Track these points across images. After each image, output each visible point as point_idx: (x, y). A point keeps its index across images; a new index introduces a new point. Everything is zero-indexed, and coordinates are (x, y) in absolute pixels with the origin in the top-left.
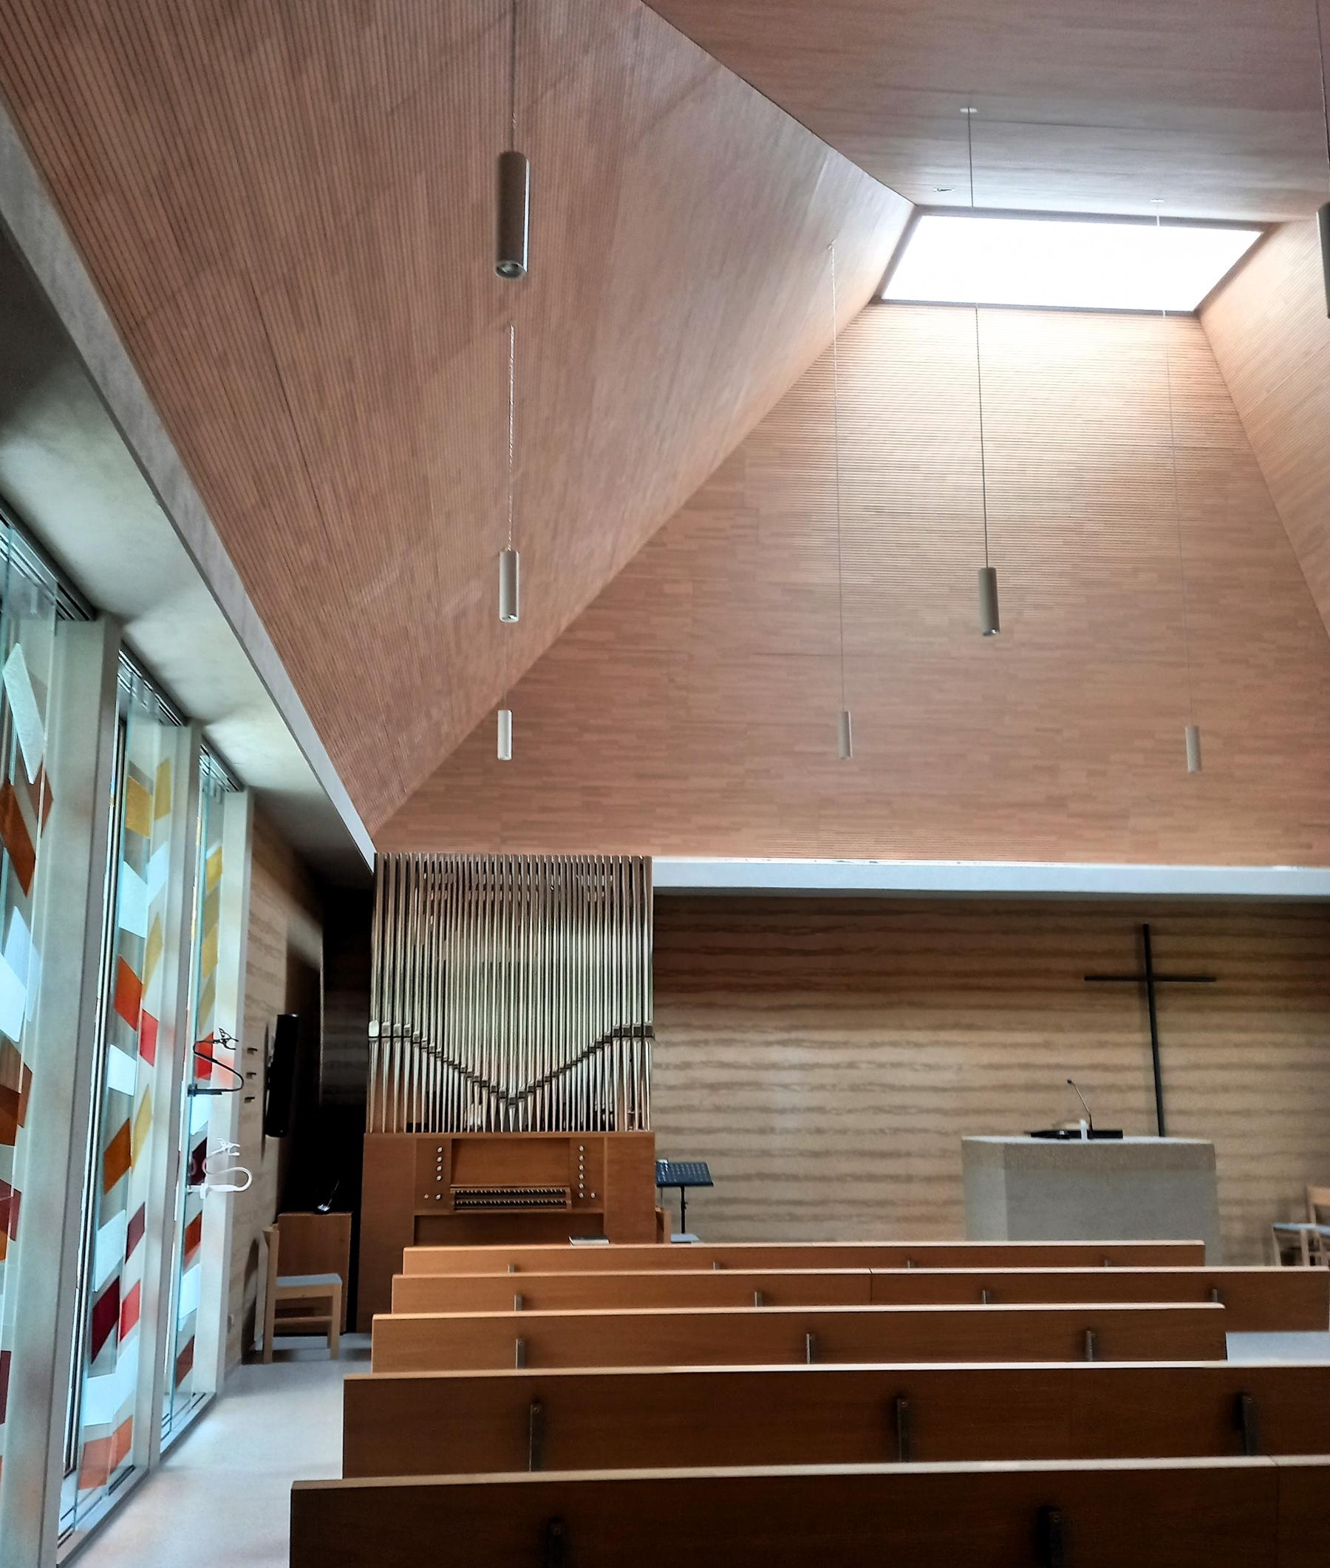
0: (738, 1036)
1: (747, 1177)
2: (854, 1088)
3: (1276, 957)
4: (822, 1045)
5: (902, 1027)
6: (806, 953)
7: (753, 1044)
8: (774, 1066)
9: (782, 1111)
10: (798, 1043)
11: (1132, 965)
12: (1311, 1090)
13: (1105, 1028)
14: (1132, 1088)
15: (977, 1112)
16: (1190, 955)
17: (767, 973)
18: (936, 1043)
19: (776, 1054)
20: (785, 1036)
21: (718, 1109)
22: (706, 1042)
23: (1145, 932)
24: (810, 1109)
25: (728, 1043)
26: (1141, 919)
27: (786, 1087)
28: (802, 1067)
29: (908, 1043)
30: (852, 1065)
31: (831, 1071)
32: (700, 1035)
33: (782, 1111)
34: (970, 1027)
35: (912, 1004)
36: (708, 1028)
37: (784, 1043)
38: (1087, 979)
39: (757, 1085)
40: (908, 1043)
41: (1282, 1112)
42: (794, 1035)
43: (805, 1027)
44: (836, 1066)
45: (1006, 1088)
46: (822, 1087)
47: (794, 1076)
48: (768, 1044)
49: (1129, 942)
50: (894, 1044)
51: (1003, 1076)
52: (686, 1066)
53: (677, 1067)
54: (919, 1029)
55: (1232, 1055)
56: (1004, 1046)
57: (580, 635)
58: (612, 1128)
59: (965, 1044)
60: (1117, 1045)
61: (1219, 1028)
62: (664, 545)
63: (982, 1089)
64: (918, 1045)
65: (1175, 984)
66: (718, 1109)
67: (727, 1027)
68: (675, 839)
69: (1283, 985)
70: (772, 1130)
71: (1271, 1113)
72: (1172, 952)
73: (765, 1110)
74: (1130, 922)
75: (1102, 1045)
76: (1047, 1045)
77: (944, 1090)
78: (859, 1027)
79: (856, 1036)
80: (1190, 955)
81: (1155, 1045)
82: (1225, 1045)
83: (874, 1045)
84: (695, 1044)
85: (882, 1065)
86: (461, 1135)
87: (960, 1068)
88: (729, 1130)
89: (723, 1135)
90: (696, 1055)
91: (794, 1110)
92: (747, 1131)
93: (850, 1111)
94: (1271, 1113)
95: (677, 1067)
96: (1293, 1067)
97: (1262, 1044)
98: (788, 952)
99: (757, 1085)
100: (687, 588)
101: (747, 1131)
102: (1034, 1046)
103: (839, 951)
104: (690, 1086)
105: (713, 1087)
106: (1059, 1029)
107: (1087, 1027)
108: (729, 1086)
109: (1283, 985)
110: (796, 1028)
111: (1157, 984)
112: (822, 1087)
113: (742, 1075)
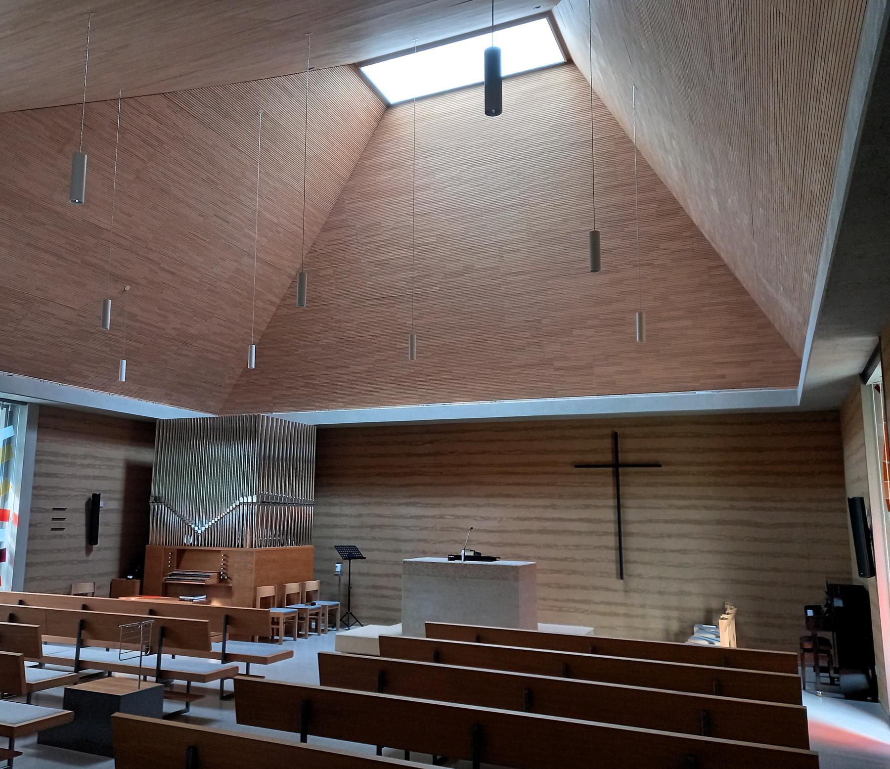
0: (385, 501)
1: (387, 575)
2: (443, 529)
3: (712, 450)
4: (426, 505)
5: (470, 496)
6: (420, 455)
7: (392, 504)
8: (402, 517)
9: (406, 541)
10: (414, 504)
11: (608, 457)
12: (733, 538)
13: (589, 496)
14: (606, 534)
15: (511, 545)
16: (649, 450)
17: (400, 467)
18: (488, 505)
19: (403, 510)
20: (408, 500)
21: (374, 539)
22: (370, 504)
23: (615, 436)
24: (419, 540)
25: (380, 504)
26: (614, 429)
27: (407, 528)
28: (417, 517)
29: (473, 504)
30: (442, 517)
31: (431, 520)
32: (367, 500)
33: (406, 541)
34: (508, 496)
35: (477, 483)
36: (370, 496)
37: (407, 504)
38: (576, 466)
39: (394, 527)
40: (473, 504)
41: (709, 552)
42: (413, 500)
43: (419, 496)
44: (433, 517)
45: (528, 531)
46: (426, 528)
47: (412, 522)
48: (400, 505)
49: (608, 443)
50: (465, 505)
51: (527, 525)
52: (361, 515)
53: (356, 516)
54: (478, 496)
55: (673, 514)
56: (528, 507)
57: (288, 301)
58: (242, 546)
59: (505, 506)
60: (596, 507)
61: (668, 497)
62: (316, 251)
63: (513, 531)
64: (478, 506)
65: (636, 469)
66: (374, 539)
67: (379, 496)
68: (350, 399)
69: (714, 468)
70: (400, 551)
71: (702, 552)
72: (630, 451)
73: (397, 540)
74: (608, 431)
75: (587, 507)
76: (553, 507)
77: (492, 532)
78: (448, 495)
79: (445, 501)
80: (649, 450)
81: (619, 507)
82: (670, 507)
83: (454, 506)
84: (364, 504)
85: (458, 517)
86: (183, 547)
87: (501, 519)
88: (379, 550)
89: (377, 553)
90: (364, 510)
91: (411, 540)
92: (388, 551)
93: (441, 542)
94: (702, 552)
95: (356, 516)
96: (719, 522)
97: (695, 507)
98: (409, 455)
99: (394, 527)
100: (330, 271)
101: (388, 551)
102: (545, 507)
103: (438, 453)
104: (361, 527)
105: (372, 527)
106: (561, 497)
107: (578, 496)
108: (380, 527)
109: (714, 468)
110: (414, 496)
111: (620, 469)
112: (426, 528)
113: (386, 521)
